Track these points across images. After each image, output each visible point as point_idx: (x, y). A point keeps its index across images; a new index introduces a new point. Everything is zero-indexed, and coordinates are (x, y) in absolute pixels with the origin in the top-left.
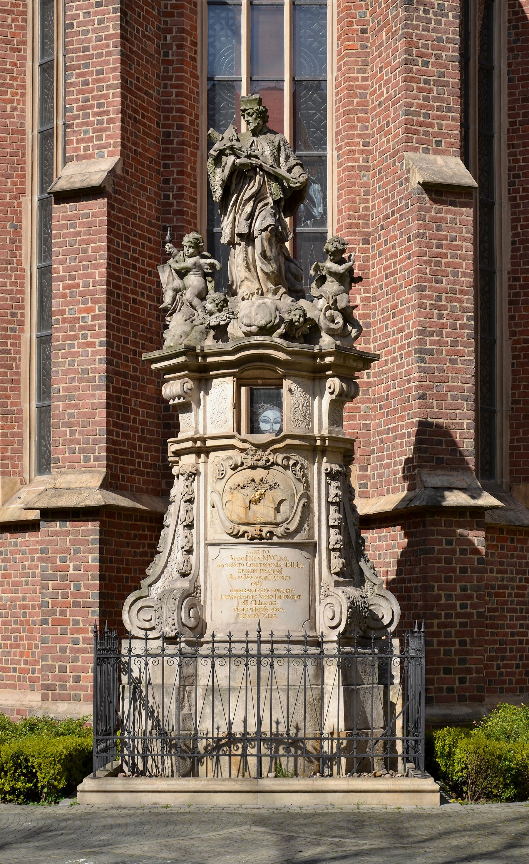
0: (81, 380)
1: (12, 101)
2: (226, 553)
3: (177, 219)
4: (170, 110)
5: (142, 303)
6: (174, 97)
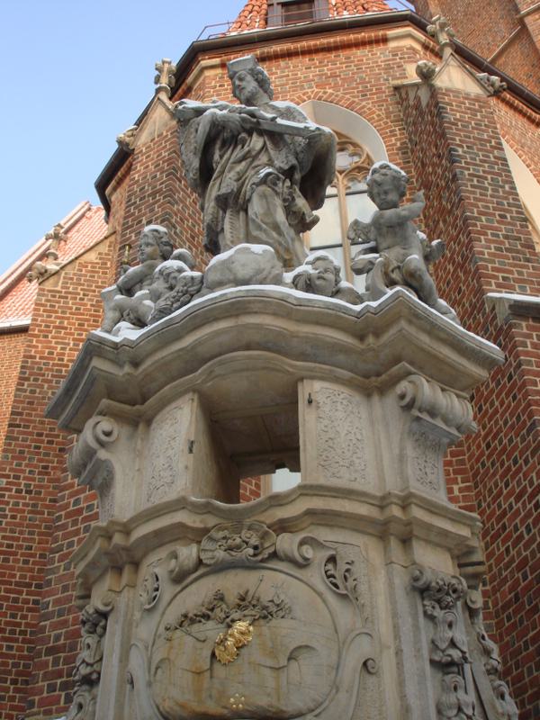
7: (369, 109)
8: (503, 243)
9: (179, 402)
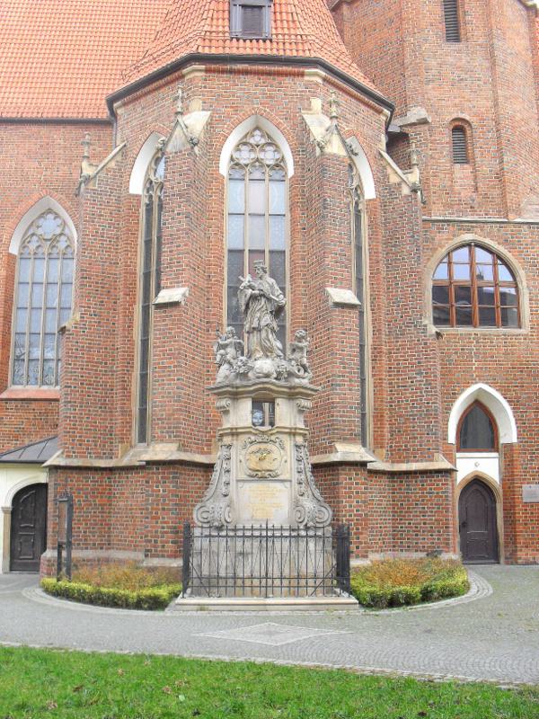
0: (167, 397)
1: (130, 258)
2: (247, 486)
5: (197, 360)
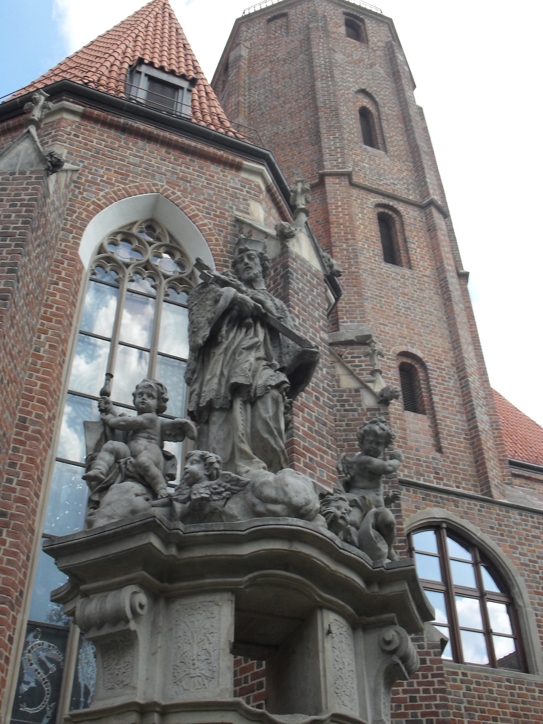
3: (17, 507)
4: (31, 399)
6: (37, 388)
7: (210, 229)
8: (313, 424)
9: (217, 597)
